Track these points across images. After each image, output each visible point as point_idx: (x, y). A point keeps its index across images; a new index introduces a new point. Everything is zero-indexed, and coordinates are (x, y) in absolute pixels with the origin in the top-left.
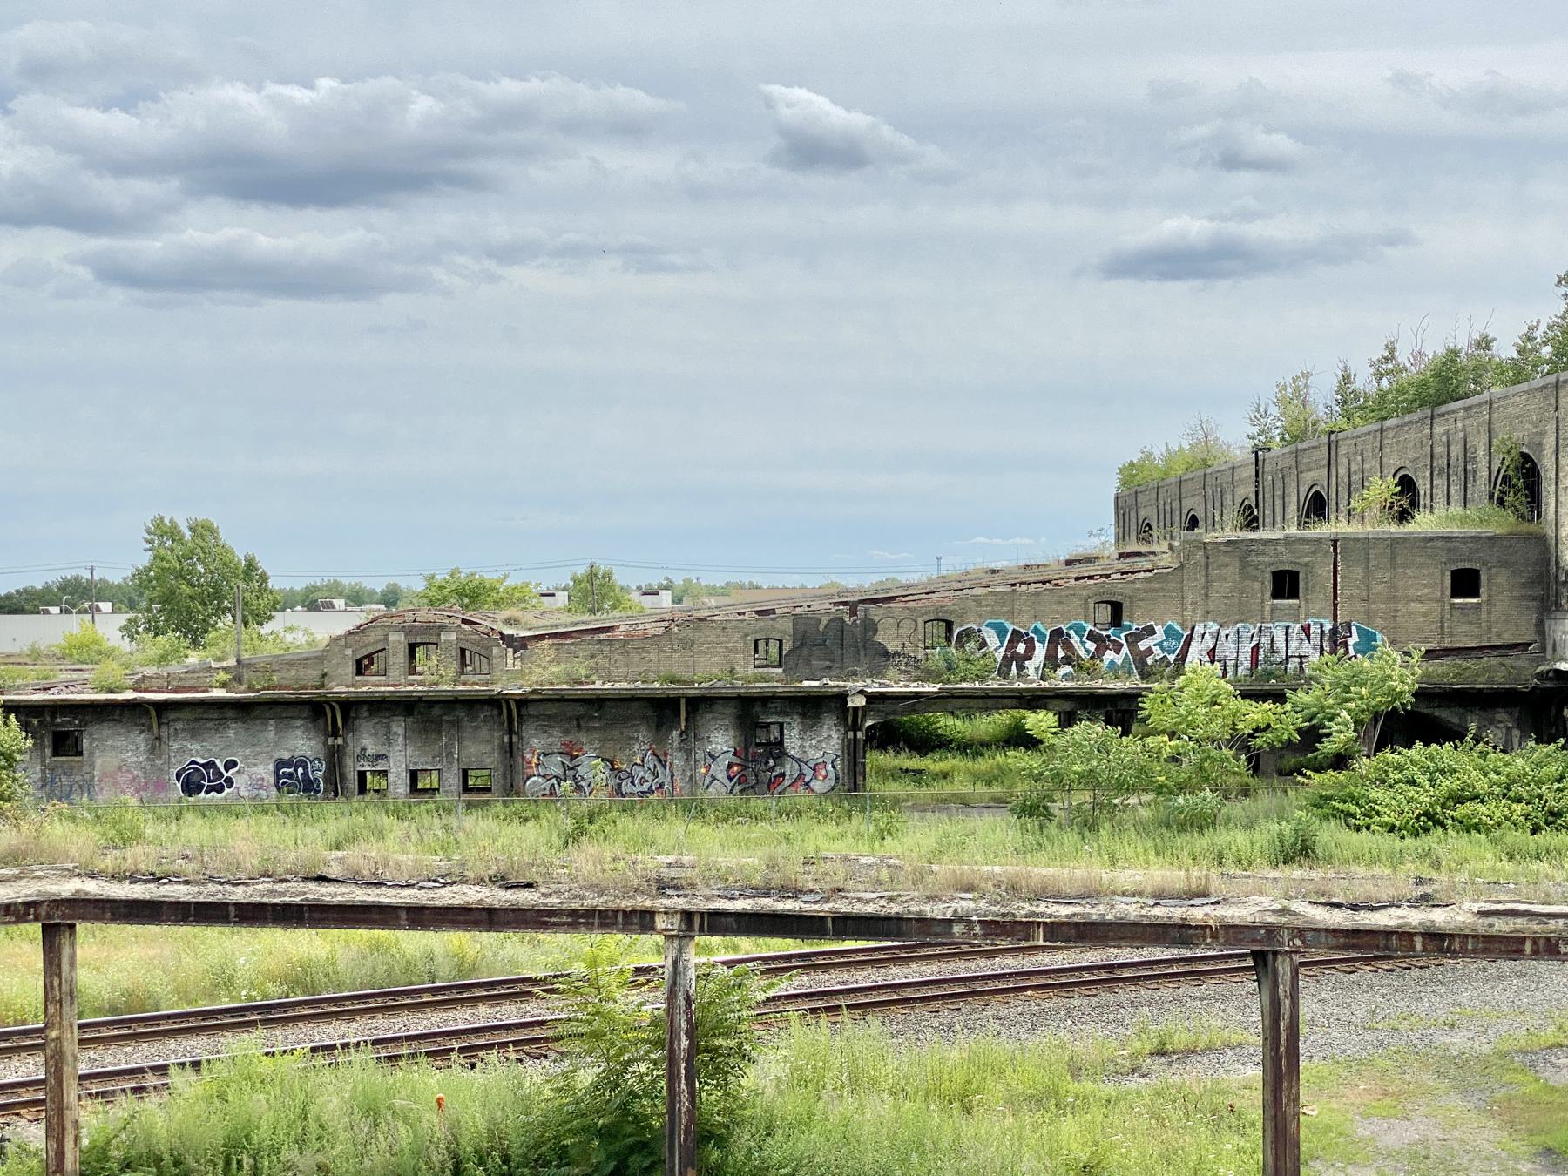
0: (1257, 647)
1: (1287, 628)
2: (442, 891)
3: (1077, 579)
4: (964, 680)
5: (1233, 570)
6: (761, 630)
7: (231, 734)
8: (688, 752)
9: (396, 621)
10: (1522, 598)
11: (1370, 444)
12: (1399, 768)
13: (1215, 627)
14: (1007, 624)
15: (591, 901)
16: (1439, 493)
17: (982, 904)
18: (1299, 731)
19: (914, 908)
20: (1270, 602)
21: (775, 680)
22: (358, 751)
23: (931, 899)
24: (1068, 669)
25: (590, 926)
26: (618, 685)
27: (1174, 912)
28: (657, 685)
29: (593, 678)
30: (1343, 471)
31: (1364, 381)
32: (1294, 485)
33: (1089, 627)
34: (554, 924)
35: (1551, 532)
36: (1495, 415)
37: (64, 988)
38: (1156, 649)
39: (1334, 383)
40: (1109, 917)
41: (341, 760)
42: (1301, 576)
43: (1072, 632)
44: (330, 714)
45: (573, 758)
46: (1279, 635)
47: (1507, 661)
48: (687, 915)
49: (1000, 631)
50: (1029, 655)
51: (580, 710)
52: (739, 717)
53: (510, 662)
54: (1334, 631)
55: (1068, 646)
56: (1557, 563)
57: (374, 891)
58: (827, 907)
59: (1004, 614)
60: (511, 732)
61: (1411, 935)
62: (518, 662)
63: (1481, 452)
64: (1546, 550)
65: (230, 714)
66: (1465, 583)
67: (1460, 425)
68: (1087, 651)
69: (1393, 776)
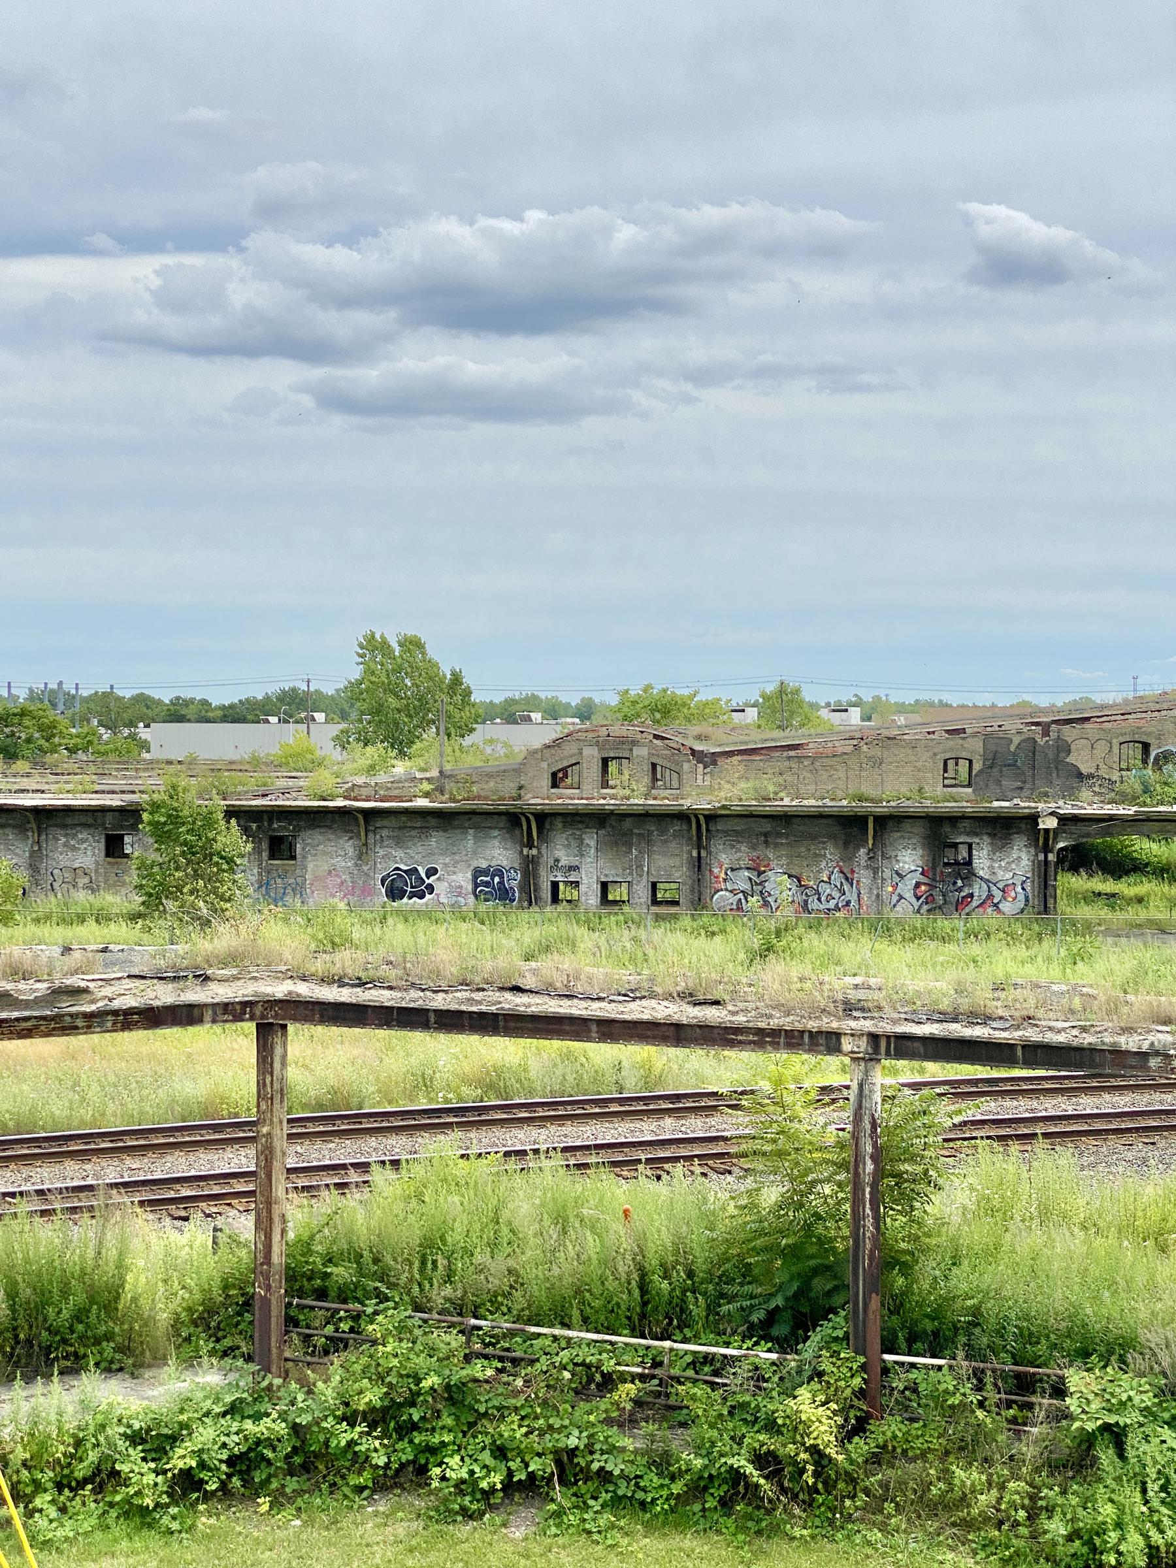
2: (633, 1005)
6: (951, 750)
7: (433, 842)
8: (875, 871)
9: (590, 735)
19: (1108, 1039)
21: (964, 800)
22: (551, 862)
23: (1127, 1030)
25: (776, 1046)
26: (806, 802)
28: (845, 803)
29: (782, 795)
34: (741, 1042)
37: (276, 1086)
41: (535, 870)
44: (527, 826)
45: (760, 874)
48: (874, 1038)
51: (767, 826)
53: (700, 777)
57: (566, 1002)
58: (1018, 1034)
60: (699, 847)
62: (707, 778)
65: (433, 822)
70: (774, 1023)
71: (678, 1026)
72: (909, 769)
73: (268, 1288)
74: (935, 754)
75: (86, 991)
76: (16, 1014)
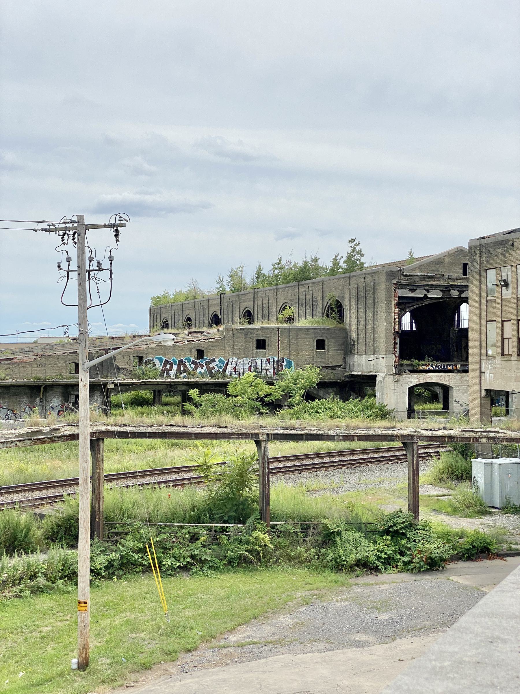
0: (251, 366)
1: (262, 360)
3: (188, 341)
4: (149, 378)
6: (72, 359)
8: (43, 406)
10: (337, 350)
12: (312, 408)
13: (236, 359)
14: (163, 358)
15: (244, 431)
16: (302, 312)
18: (281, 395)
20: (255, 350)
23: (330, 429)
24: (185, 374)
25: (242, 438)
26: (18, 380)
28: (32, 380)
29: (7, 378)
30: (260, 303)
31: (267, 270)
32: (237, 307)
33: (192, 359)
34: (233, 438)
35: (348, 327)
36: (325, 286)
37: (101, 458)
38: (216, 367)
39: (255, 270)
40: (374, 434)
42: (267, 341)
43: (186, 361)
46: (259, 362)
47: (333, 371)
48: (268, 435)
49: (161, 360)
50: (171, 369)
52: (63, 393)
54: (278, 361)
55: (185, 366)
56: (350, 339)
57: (186, 429)
59: (162, 354)
61: (445, 437)
63: (319, 299)
66: (320, 344)
67: (310, 288)
68: (192, 368)
69: (311, 411)
70: (242, 432)
71: (217, 434)
72: (56, 367)
73: (99, 519)
74: (66, 361)
75: (59, 429)
76: (43, 437)
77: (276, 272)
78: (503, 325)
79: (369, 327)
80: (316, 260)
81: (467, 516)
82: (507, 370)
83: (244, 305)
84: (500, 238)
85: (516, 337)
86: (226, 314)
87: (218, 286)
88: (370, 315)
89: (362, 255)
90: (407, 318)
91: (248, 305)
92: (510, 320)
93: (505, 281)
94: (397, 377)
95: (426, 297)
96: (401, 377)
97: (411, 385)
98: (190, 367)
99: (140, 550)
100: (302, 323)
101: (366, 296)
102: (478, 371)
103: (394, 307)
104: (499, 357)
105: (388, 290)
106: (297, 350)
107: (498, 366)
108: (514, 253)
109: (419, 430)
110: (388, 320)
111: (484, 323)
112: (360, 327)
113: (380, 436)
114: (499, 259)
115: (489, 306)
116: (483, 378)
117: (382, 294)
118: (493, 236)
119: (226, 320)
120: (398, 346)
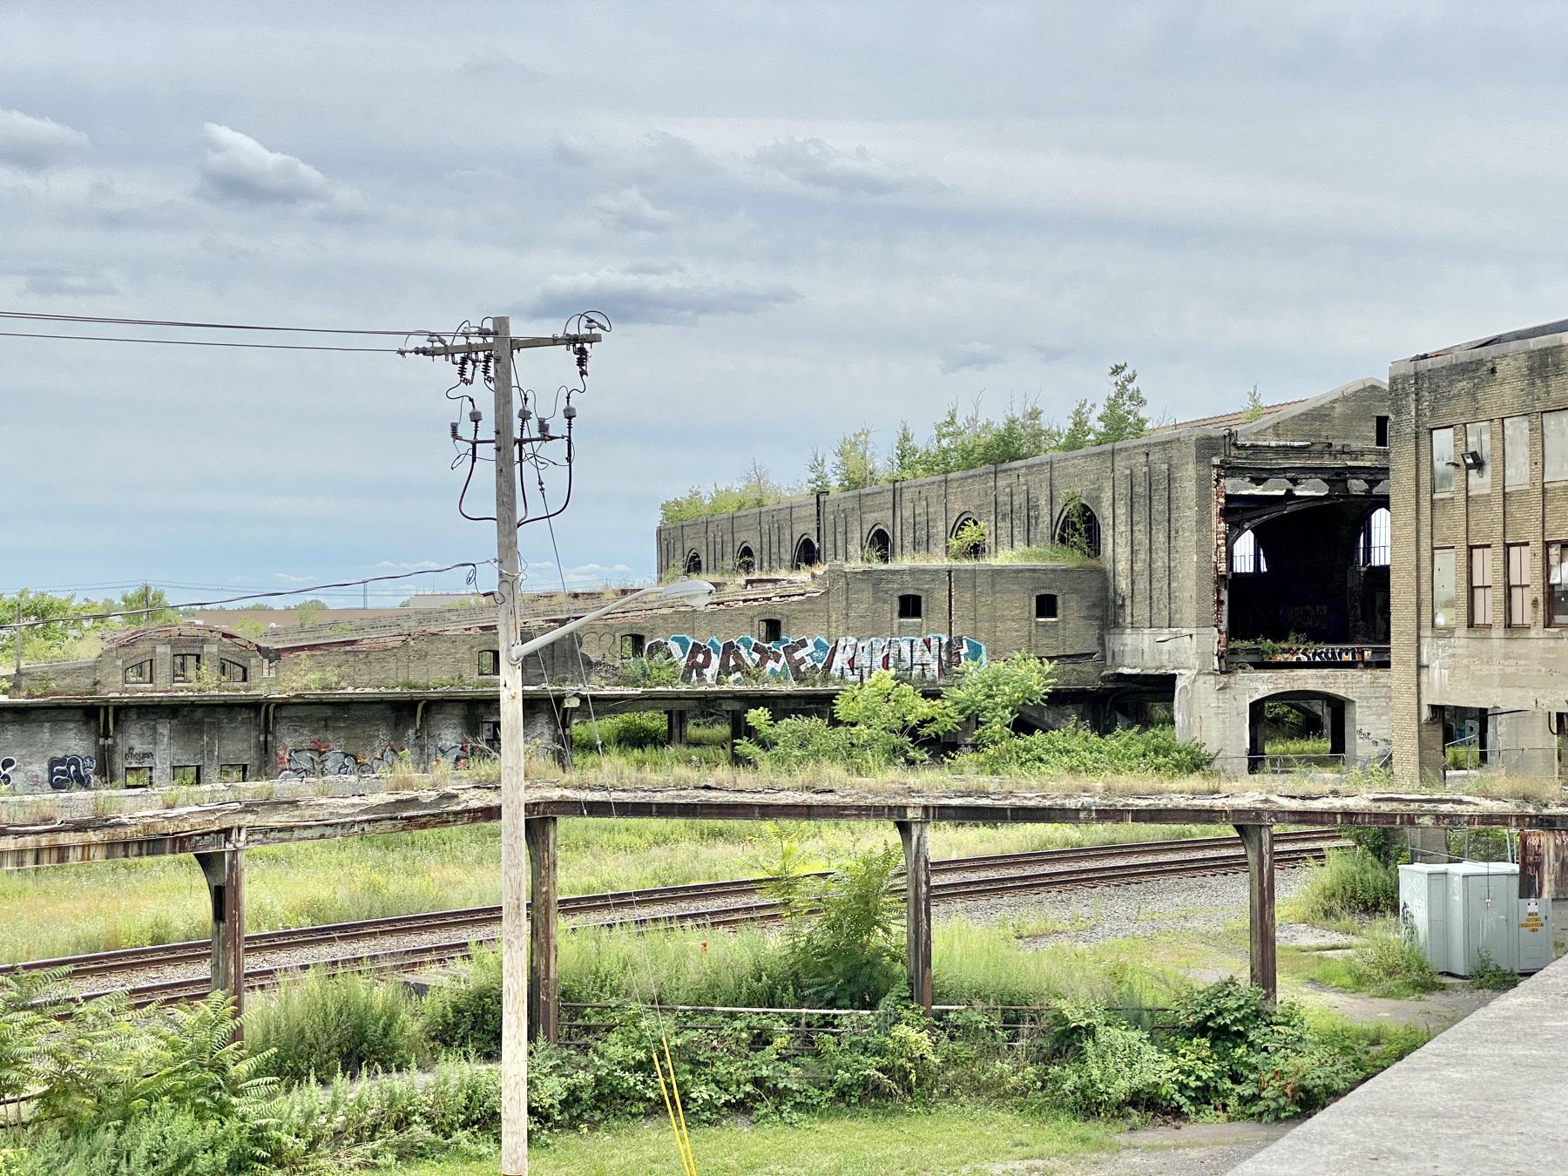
4: (658, 684)
5: (867, 595)
7: (9, 735)
8: (422, 748)
9: (163, 635)
11: (934, 492)
12: (1028, 750)
13: (854, 641)
15: (871, 800)
17: (1097, 799)
20: (897, 621)
22: (126, 750)
23: (1068, 796)
24: (738, 675)
25: (868, 816)
26: (367, 690)
27: (1206, 803)
28: (398, 690)
29: (343, 684)
30: (907, 513)
32: (857, 524)
33: (754, 641)
35: (1109, 566)
38: (808, 659)
41: (110, 759)
44: (100, 717)
45: (321, 754)
47: (1078, 667)
48: (926, 808)
49: (683, 643)
50: (706, 664)
51: (329, 712)
52: (466, 717)
53: (266, 671)
54: (949, 644)
55: (738, 656)
60: (267, 732)
62: (273, 671)
64: (1106, 579)
65: (9, 717)
66: (1046, 606)
67: (1022, 480)
69: (1024, 756)
70: (869, 802)
71: (810, 807)
72: (450, 660)
73: (548, 995)
75: (456, 796)
76: (421, 813)
77: (945, 443)
78: (1470, 557)
79: (1158, 564)
80: (1034, 415)
81: (1388, 994)
82: (1481, 659)
83: (871, 518)
84: (1464, 357)
85: (1501, 585)
86: (830, 538)
87: (813, 476)
88: (1160, 537)
89: (1142, 402)
90: (1245, 545)
91: (881, 517)
92: (1488, 546)
93: (1474, 455)
94: (1224, 678)
95: (1289, 495)
96: (1232, 680)
97: (1257, 697)
98: (750, 658)
99: (640, 1066)
100: (1003, 558)
101: (1150, 495)
102: (1413, 663)
103: (1214, 520)
104: (1462, 631)
105: (1202, 483)
106: (993, 619)
107: (1460, 651)
108: (1495, 390)
109: (1273, 797)
110: (1201, 547)
111: (1426, 554)
112: (1138, 567)
113: (1184, 810)
114: (1462, 405)
115: (1437, 514)
116: (1424, 678)
117: (1187, 487)
118: (1448, 351)
119: (830, 552)
120: (1225, 607)
